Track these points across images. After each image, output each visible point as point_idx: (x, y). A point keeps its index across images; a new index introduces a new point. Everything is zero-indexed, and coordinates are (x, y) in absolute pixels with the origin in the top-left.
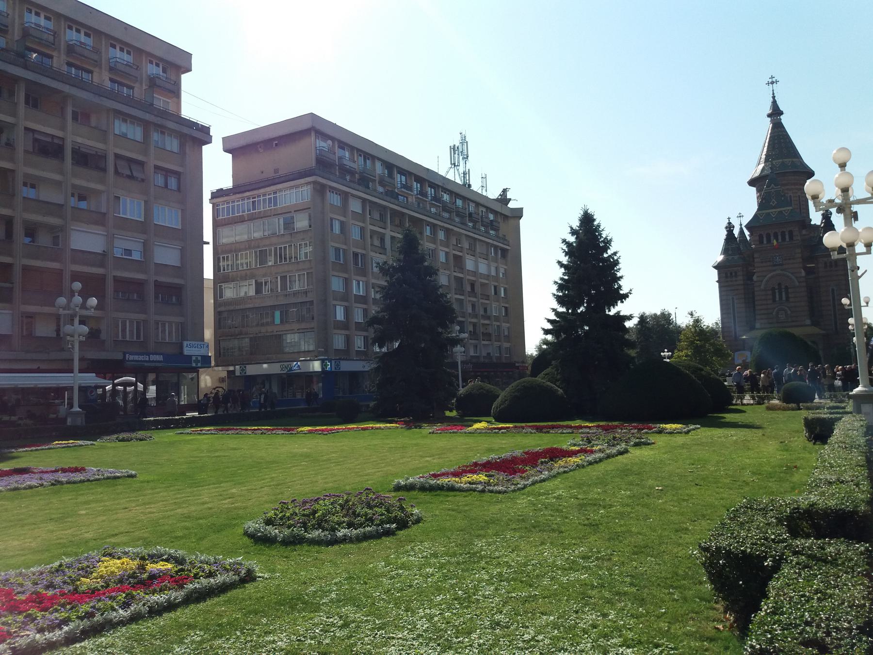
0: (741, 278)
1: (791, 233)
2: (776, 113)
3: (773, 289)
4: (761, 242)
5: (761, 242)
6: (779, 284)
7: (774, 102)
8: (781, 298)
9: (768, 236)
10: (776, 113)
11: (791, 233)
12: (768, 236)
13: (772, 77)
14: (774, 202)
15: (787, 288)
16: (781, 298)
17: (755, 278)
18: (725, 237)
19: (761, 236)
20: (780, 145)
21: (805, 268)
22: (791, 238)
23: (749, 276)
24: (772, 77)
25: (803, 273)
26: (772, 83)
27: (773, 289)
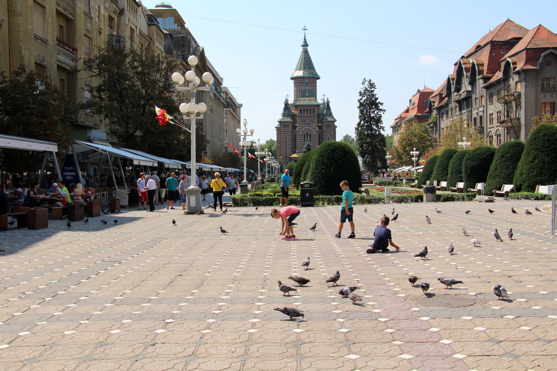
0: (290, 128)
1: (314, 110)
2: (305, 45)
3: (305, 135)
4: (301, 112)
5: (301, 112)
6: (307, 133)
7: (305, 39)
8: (307, 139)
9: (304, 110)
10: (305, 45)
11: (314, 110)
12: (304, 110)
13: (305, 27)
14: (307, 94)
15: (310, 135)
16: (307, 139)
17: (297, 129)
18: (283, 107)
19: (301, 110)
20: (307, 62)
21: (318, 126)
22: (314, 112)
23: (294, 127)
24: (305, 27)
25: (318, 129)
26: (305, 30)
27: (305, 135)
